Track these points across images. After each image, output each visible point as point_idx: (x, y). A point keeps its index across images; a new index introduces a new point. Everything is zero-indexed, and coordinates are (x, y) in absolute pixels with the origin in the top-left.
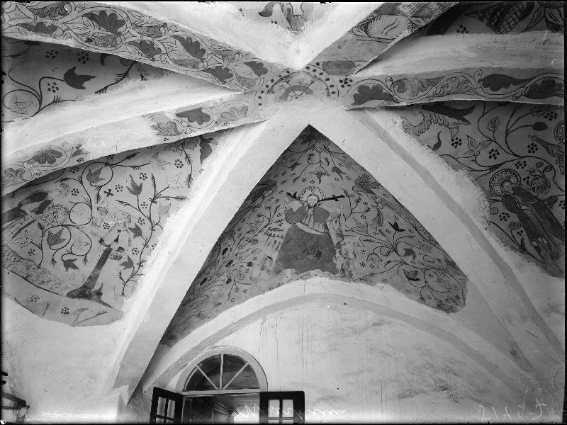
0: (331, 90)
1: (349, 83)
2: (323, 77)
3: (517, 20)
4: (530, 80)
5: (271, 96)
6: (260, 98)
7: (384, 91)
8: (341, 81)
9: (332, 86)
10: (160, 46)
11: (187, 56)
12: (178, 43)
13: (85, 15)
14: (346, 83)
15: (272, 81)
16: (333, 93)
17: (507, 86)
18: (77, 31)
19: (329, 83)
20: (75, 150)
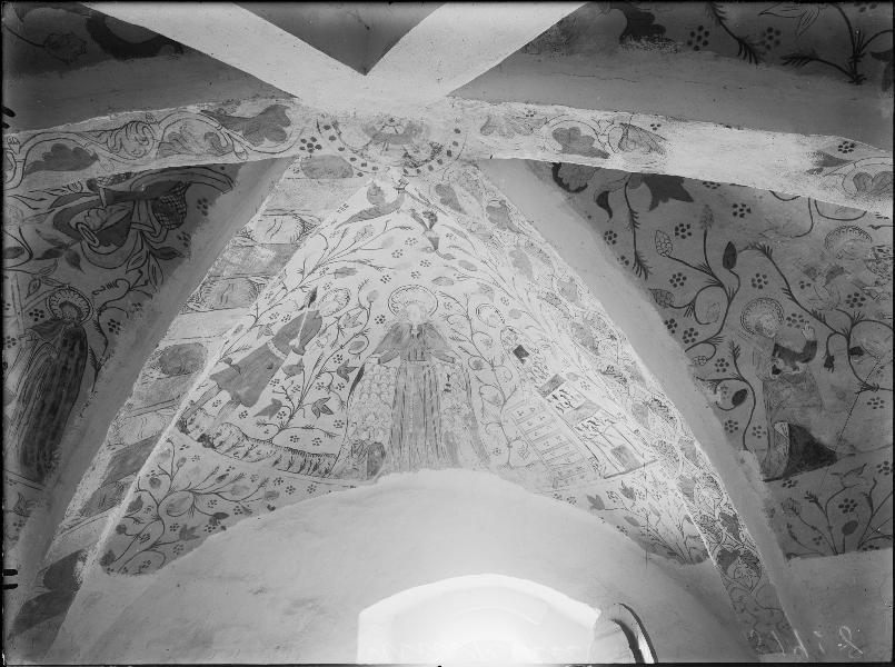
0: (332, 132)
1: (305, 145)
2: (348, 155)
5: (436, 139)
6: (455, 144)
7: (240, 133)
8: (319, 147)
9: (332, 138)
14: (310, 145)
15: (431, 168)
16: (327, 128)
17: (46, 156)
19: (338, 144)
20: (827, 170)
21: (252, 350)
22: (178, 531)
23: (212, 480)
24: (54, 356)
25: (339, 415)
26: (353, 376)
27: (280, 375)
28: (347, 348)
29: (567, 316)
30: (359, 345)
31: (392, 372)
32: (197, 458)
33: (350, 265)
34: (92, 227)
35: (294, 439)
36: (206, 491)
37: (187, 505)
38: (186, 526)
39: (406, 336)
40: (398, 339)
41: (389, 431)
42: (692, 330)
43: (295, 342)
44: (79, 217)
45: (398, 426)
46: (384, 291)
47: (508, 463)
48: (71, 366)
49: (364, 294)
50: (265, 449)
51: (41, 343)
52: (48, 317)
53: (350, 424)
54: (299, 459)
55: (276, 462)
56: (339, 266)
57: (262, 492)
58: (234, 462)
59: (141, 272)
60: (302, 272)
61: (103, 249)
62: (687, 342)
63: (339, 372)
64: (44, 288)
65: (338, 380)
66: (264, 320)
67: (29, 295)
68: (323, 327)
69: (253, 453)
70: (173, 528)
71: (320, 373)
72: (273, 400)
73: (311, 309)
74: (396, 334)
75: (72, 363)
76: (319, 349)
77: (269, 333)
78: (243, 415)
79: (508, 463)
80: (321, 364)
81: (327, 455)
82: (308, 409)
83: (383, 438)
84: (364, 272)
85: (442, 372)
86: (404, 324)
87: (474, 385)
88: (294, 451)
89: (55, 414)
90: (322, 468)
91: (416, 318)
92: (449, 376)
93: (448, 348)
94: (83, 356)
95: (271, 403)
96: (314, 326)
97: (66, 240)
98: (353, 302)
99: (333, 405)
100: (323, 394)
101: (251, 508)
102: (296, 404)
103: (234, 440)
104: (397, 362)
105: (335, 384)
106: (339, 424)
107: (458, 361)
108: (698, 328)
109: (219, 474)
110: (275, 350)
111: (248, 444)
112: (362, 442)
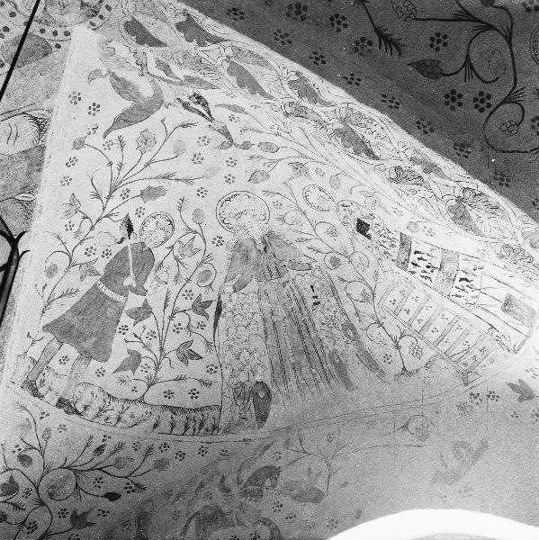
10: (289, 91)
11: (252, 69)
12: (267, 91)
13: (377, 158)
18: (388, 145)
21: (81, 294)
22: (68, 516)
23: (90, 452)
25: (210, 358)
26: (211, 311)
27: (125, 320)
28: (194, 279)
29: (321, 124)
30: (207, 274)
31: (252, 299)
32: (62, 428)
33: (154, 184)
35: (169, 394)
36: (86, 467)
37: (69, 487)
38: (75, 512)
39: (253, 254)
40: (246, 257)
41: (268, 366)
42: (481, 94)
43: (129, 281)
45: (276, 359)
46: (208, 206)
47: (404, 369)
49: (188, 215)
50: (139, 410)
53: (223, 367)
54: (181, 418)
55: (156, 426)
56: (144, 185)
57: (151, 460)
58: (108, 429)
60: (98, 196)
62: (482, 110)
63: (194, 308)
65: (196, 318)
66: (79, 256)
68: (158, 259)
69: (126, 416)
70: (63, 513)
71: (173, 314)
72: (129, 351)
73: (132, 241)
74: (241, 252)
76: (163, 286)
77: (93, 272)
78: (100, 373)
79: (404, 369)
80: (170, 303)
81: (208, 407)
82: (173, 356)
83: (263, 375)
84: (175, 190)
85: (304, 281)
86: (244, 237)
87: (339, 286)
88: (173, 409)
90: (208, 424)
91: (257, 232)
92: (312, 287)
93: (300, 254)
95: (128, 356)
96: (145, 259)
98: (179, 226)
99: (198, 347)
100: (184, 337)
101: (142, 483)
102: (158, 354)
103: (98, 404)
104: (253, 285)
105: (194, 324)
106: (211, 370)
107: (314, 265)
108: (488, 89)
109: (93, 447)
110: (108, 292)
111: (117, 406)
112: (243, 385)
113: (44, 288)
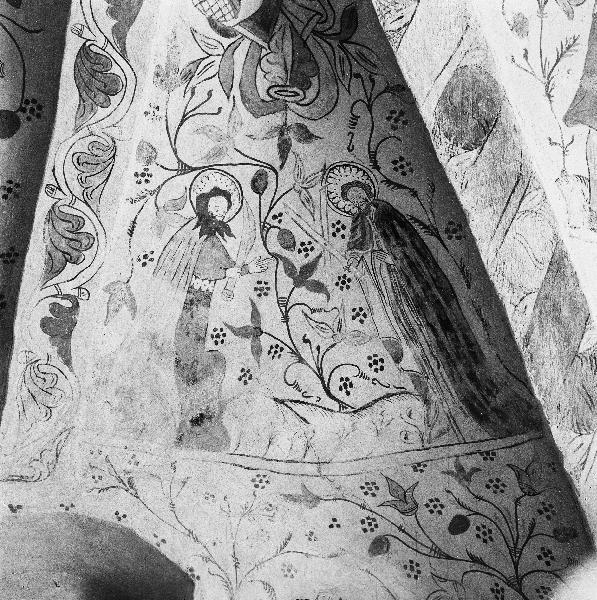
3: (210, 13)
4: (123, 54)
24: (389, 260)
34: (281, 83)
44: (262, 85)
48: (415, 256)
51: (367, 259)
52: (348, 221)
59: (358, 76)
61: (311, 93)
64: (315, 193)
67: (312, 214)
75: (409, 250)
89: (452, 330)
94: (413, 234)
97: (276, 120)
113: (526, 56)
